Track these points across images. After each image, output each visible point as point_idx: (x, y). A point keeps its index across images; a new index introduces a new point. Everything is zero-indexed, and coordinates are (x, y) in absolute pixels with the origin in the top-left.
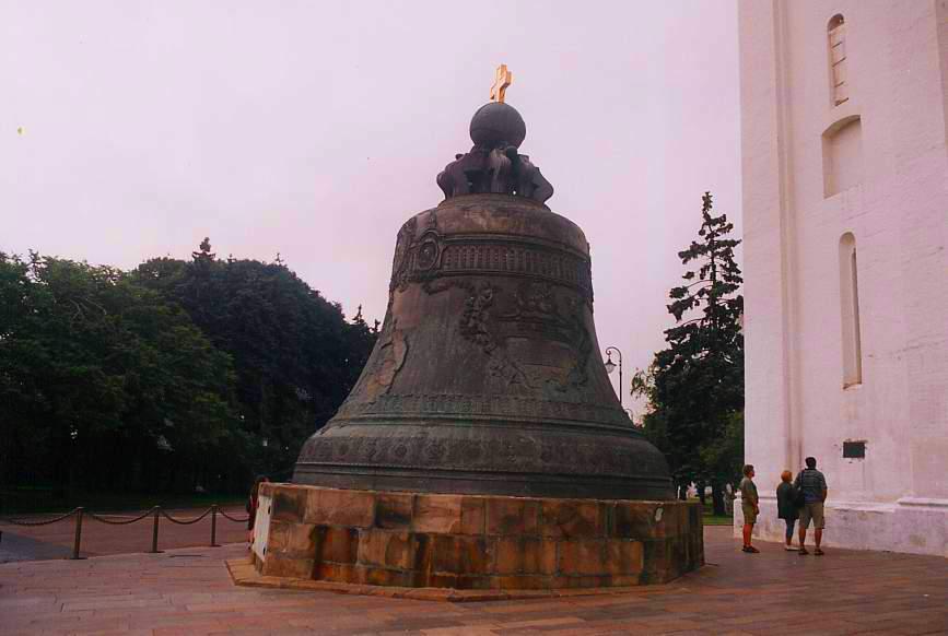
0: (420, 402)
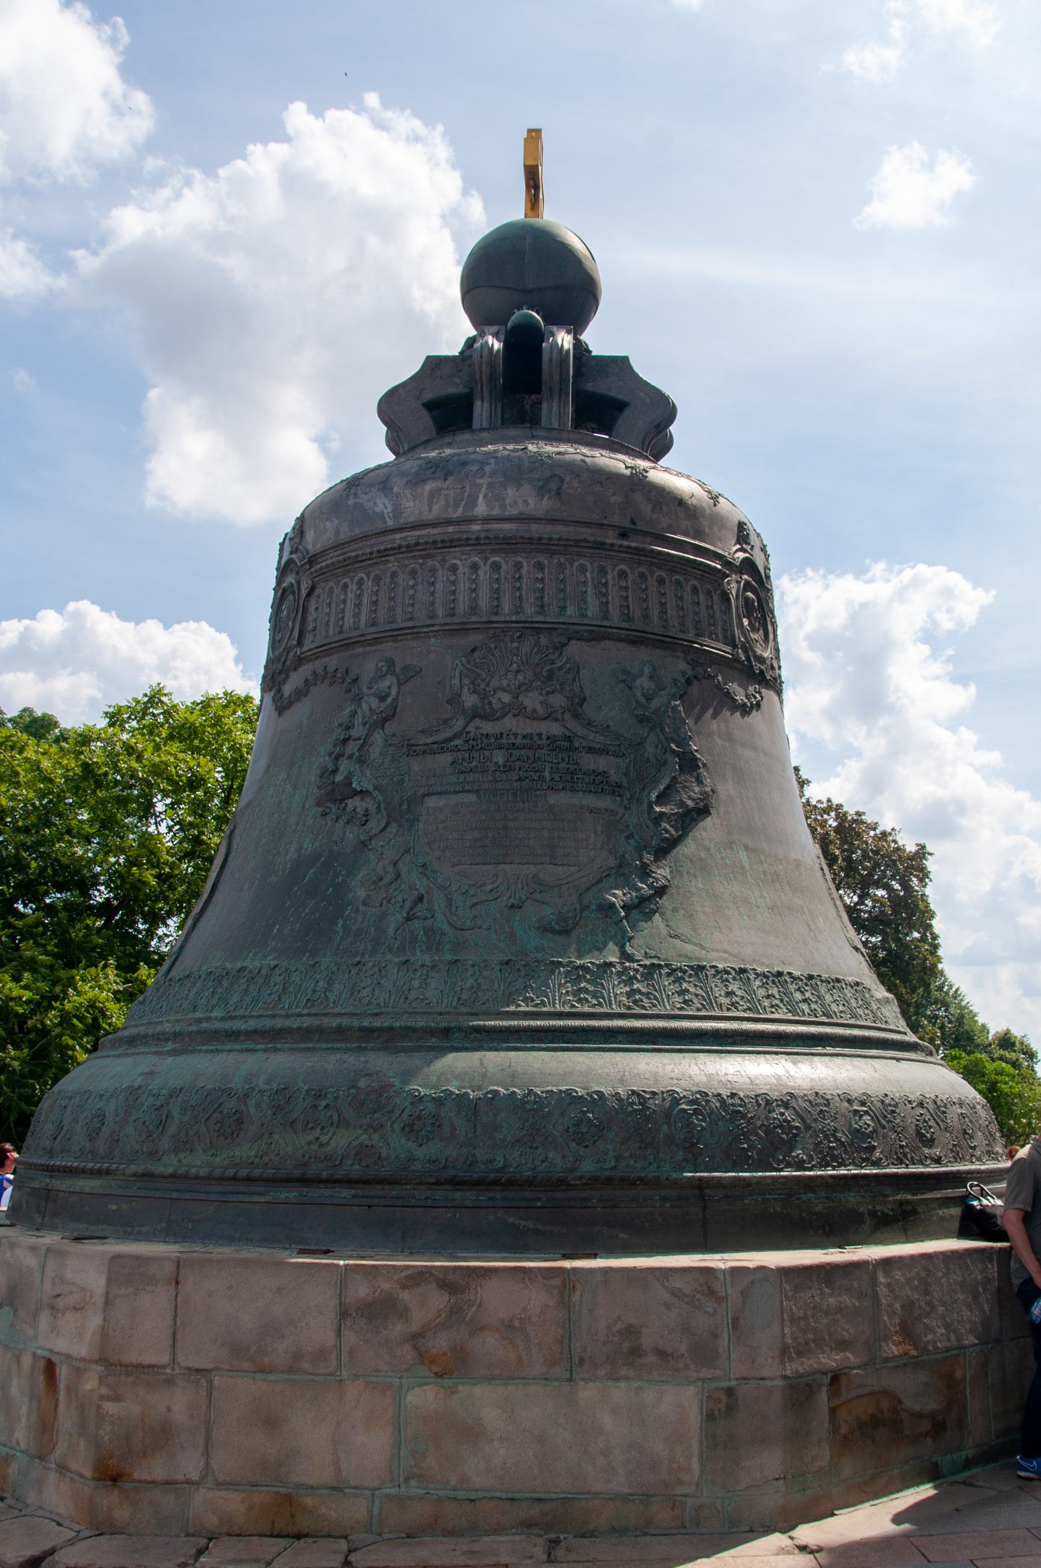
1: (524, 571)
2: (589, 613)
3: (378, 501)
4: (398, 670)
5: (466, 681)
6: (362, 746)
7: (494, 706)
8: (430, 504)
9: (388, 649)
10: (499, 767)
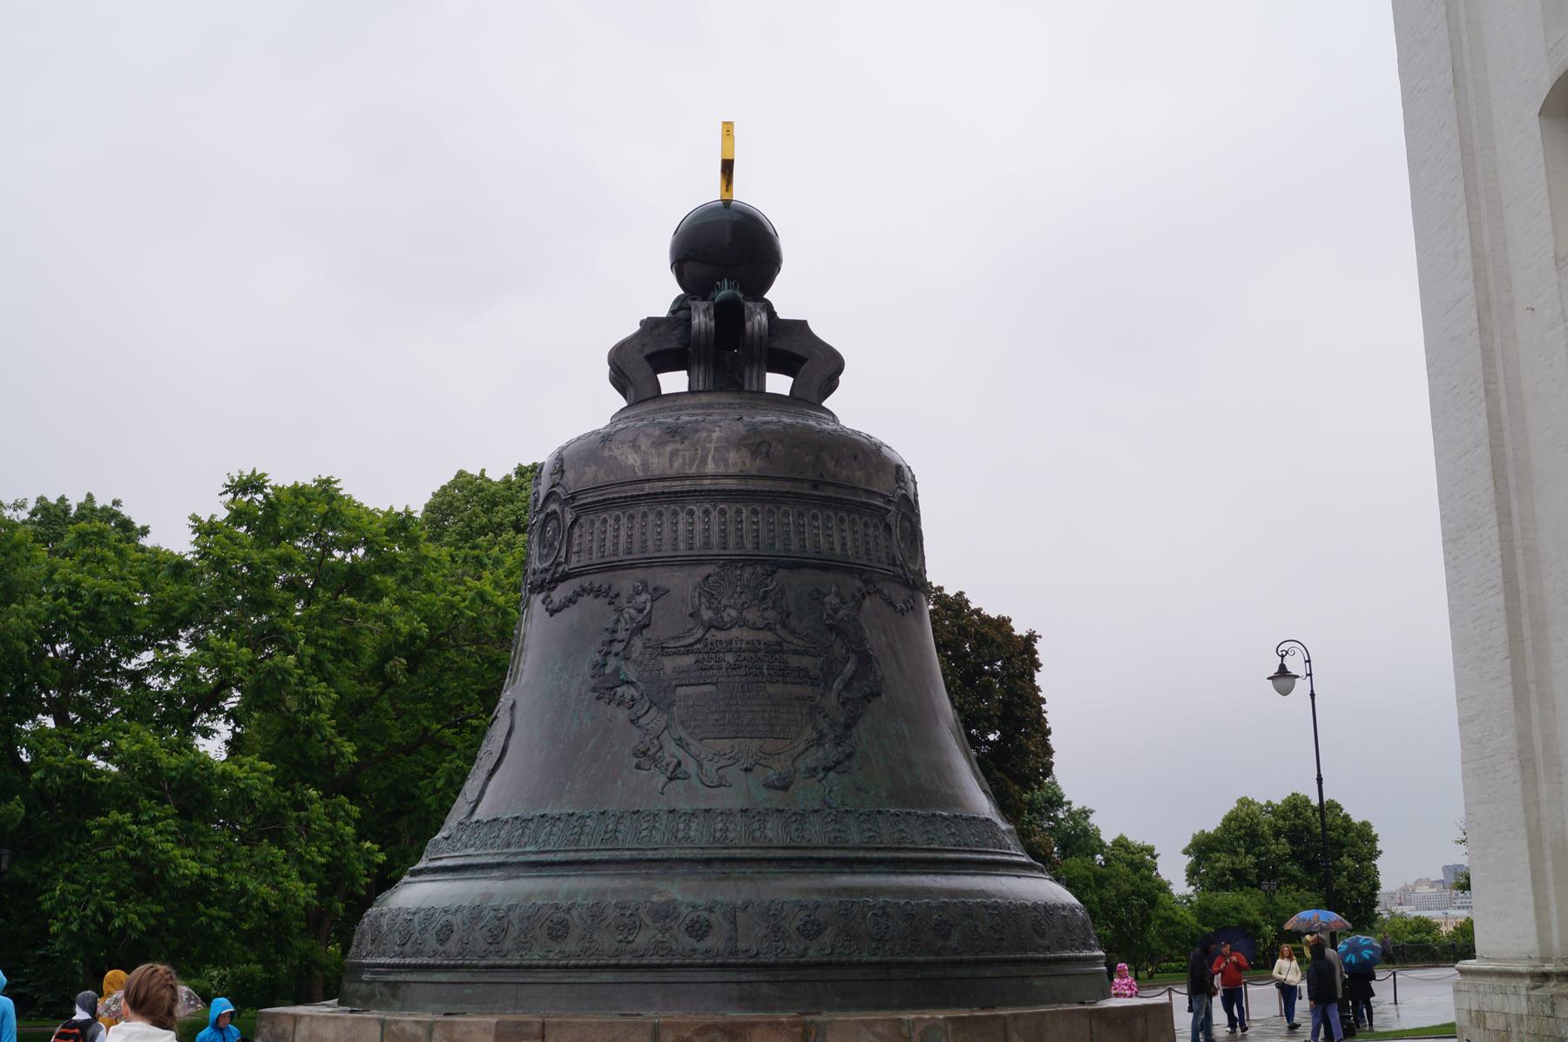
0: (508, 827)
1: (744, 516)
2: (792, 548)
3: (629, 456)
4: (650, 590)
5: (703, 600)
7: (725, 619)
8: (671, 460)
9: (641, 574)
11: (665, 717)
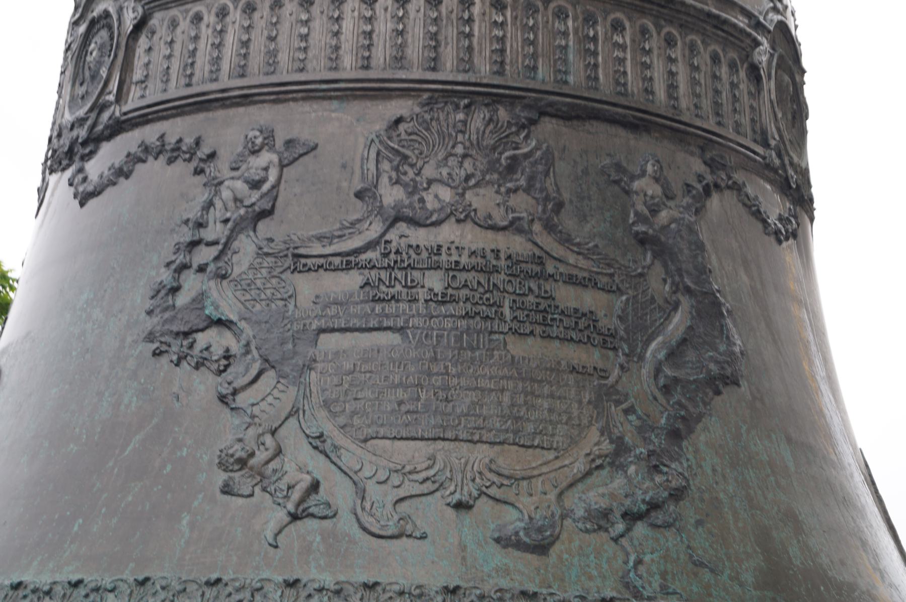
2: (571, 79)
4: (279, 143)
5: (386, 166)
6: (222, 252)
7: (429, 206)
10: (436, 295)
11: (293, 391)
